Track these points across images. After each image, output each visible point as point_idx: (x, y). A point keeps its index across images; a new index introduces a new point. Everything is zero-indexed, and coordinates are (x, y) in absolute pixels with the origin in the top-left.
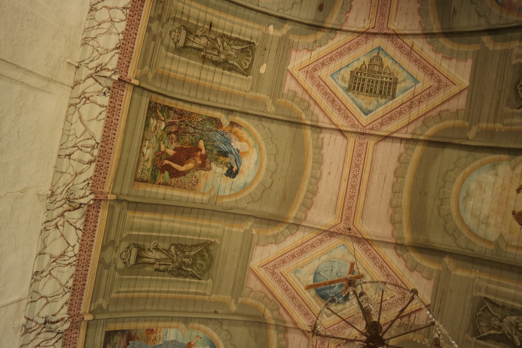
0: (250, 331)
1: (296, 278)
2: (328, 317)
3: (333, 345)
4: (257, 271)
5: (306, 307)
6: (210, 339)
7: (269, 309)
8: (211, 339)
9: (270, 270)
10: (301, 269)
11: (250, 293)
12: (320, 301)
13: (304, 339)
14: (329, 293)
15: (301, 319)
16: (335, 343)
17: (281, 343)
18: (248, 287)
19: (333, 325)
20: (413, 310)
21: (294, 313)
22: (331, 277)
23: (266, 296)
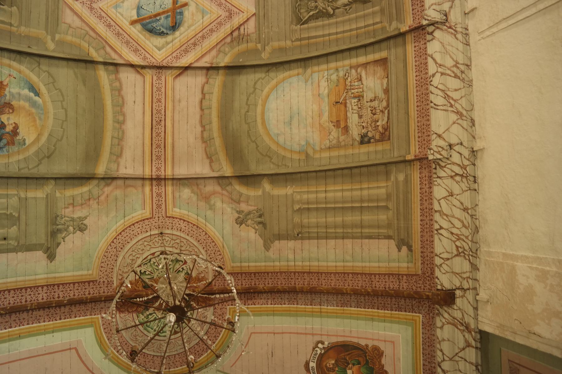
0: (75, 74)
1: (117, 13)
2: (159, 50)
3: (170, 78)
4: (71, 4)
5: (134, 43)
6: (27, 81)
7: (93, 47)
8: (28, 80)
9: (87, 5)
10: (121, 4)
11: (68, 30)
12: (148, 35)
13: (138, 77)
14: (156, 26)
15: (132, 56)
16: (172, 76)
17: (114, 85)
18: (65, 23)
19: (166, 58)
20: (241, 23)
21: (122, 51)
22: (155, 10)
23: (87, 33)
